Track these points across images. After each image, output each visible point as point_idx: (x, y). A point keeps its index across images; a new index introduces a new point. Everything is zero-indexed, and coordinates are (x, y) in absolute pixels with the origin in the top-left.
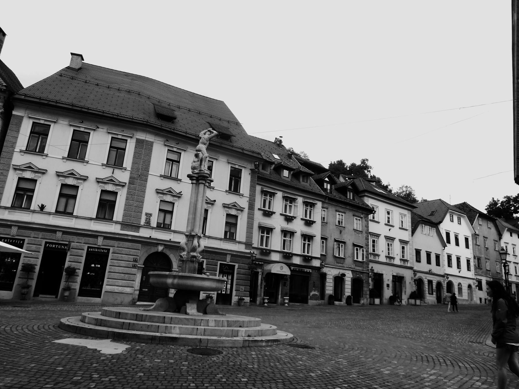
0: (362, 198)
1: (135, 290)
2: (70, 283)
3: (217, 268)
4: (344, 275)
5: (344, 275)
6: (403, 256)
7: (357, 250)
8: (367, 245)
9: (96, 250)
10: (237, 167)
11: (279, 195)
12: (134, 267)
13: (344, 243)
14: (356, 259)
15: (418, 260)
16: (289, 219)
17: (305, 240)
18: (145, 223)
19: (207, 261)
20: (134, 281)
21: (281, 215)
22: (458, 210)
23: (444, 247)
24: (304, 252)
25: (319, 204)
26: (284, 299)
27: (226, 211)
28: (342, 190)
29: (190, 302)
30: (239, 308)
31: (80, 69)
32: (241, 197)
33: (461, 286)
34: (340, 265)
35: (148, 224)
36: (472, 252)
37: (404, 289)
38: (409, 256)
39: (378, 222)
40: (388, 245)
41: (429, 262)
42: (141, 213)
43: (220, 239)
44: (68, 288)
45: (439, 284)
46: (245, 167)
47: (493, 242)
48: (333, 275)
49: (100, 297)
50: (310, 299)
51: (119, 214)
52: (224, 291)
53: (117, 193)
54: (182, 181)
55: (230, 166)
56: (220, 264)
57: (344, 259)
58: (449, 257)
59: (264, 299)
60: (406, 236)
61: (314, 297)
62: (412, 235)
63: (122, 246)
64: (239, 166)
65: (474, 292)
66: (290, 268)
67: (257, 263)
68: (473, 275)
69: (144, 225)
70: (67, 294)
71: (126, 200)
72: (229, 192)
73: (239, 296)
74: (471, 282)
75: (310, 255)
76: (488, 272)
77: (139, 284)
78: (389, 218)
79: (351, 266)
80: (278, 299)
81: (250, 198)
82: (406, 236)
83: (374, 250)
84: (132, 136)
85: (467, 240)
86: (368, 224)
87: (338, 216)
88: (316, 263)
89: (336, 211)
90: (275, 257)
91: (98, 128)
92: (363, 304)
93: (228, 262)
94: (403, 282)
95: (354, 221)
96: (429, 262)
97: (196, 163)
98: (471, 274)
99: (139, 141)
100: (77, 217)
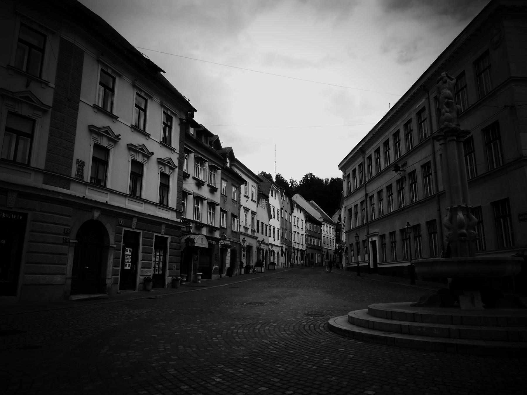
1: (66, 278)
7: (234, 219)
9: (4, 216)
11: (192, 155)
12: (66, 242)
14: (233, 230)
16: (199, 184)
18: (77, 175)
19: (143, 233)
20: (65, 264)
23: (270, 219)
25: (219, 172)
27: (161, 168)
35: (80, 179)
37: (252, 258)
41: (262, 233)
42: (72, 159)
45: (266, 251)
50: (213, 274)
52: (157, 271)
54: (119, 119)
58: (270, 227)
64: (172, 112)
73: (173, 276)
77: (72, 269)
79: (230, 237)
80: (191, 275)
81: (180, 155)
88: (217, 234)
92: (236, 274)
93: (162, 234)
98: (278, 243)
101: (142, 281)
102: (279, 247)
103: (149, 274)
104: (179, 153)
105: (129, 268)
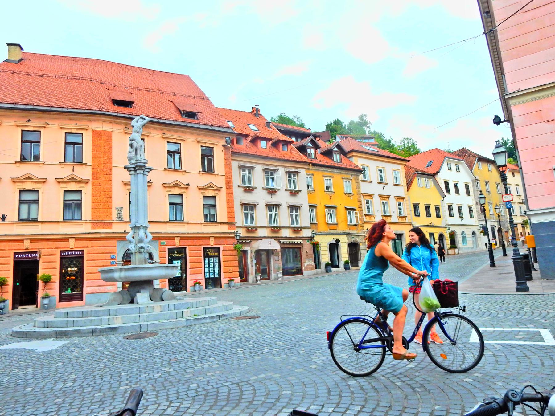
0: (350, 159)
2: (47, 291)
3: (201, 253)
4: (338, 241)
5: (338, 241)
6: (400, 213)
7: (350, 213)
8: (360, 207)
10: (207, 145)
11: (259, 168)
13: (335, 208)
14: (349, 223)
15: (417, 215)
16: (272, 192)
17: (292, 211)
21: (263, 188)
22: (457, 157)
23: (444, 198)
24: (292, 223)
25: (303, 172)
26: (277, 275)
28: (328, 153)
29: (142, 292)
30: (230, 289)
31: (21, 60)
32: (216, 176)
33: (465, 234)
34: (333, 231)
35: (120, 220)
36: (474, 199)
38: (406, 212)
39: (371, 182)
40: (384, 203)
41: (428, 215)
43: (201, 223)
44: (47, 297)
45: (441, 236)
46: (216, 145)
47: (495, 185)
48: (327, 242)
49: (82, 300)
50: (306, 270)
51: (87, 212)
53: (81, 191)
55: (200, 145)
56: (204, 248)
57: (337, 224)
59: (256, 277)
60: (401, 191)
61: (309, 268)
62: (408, 190)
63: (97, 245)
65: (479, 239)
66: (280, 242)
67: (244, 241)
68: (476, 221)
69: (116, 220)
70: (46, 301)
71: (93, 196)
72: (203, 174)
74: (475, 229)
75: (299, 225)
76: (492, 216)
78: (381, 176)
81: (226, 176)
82: (401, 191)
83: (369, 211)
84: (87, 128)
85: (467, 187)
86: (359, 185)
87: (325, 181)
88: (306, 233)
89: (323, 176)
90: (261, 233)
91: (48, 124)
94: (403, 239)
95: (343, 185)
96: (428, 215)
97: (131, 153)
99: (95, 133)
100: (42, 222)
101: (193, 284)
102: (478, 226)
103: (199, 278)
104: (224, 175)
105: (180, 275)
